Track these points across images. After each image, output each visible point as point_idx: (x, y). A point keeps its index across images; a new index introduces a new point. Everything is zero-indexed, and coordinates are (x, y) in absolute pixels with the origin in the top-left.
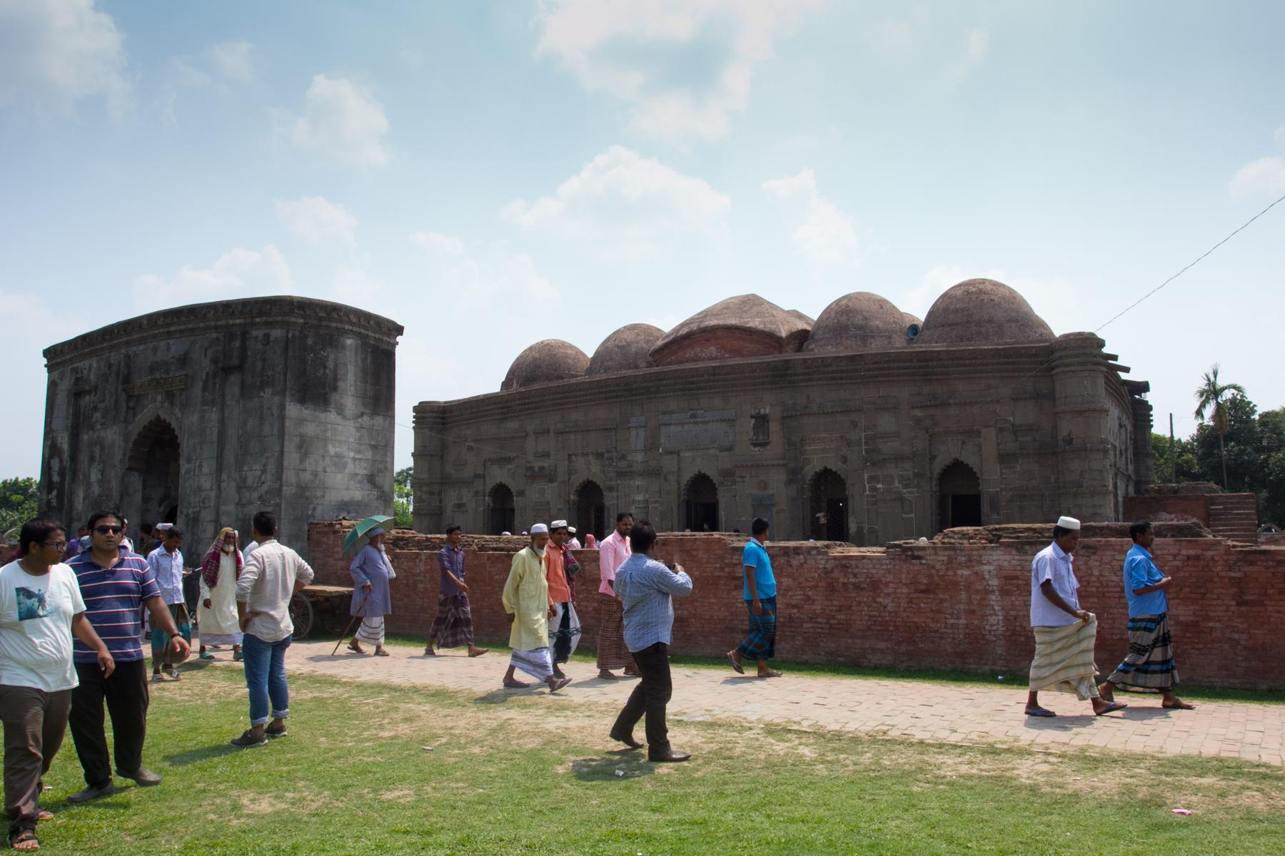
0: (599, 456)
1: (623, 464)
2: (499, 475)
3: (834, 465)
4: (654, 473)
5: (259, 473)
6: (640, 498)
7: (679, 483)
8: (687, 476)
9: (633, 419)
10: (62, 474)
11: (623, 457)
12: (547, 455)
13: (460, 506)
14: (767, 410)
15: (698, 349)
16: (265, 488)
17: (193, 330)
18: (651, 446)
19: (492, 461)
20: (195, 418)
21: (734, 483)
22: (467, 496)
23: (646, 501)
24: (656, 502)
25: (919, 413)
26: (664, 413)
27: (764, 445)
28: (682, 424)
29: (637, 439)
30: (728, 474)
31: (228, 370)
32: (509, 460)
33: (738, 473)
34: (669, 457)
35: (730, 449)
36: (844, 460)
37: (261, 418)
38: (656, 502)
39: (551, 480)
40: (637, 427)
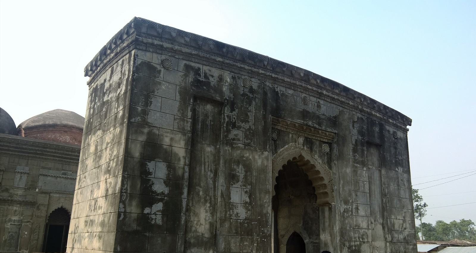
5: (401, 222)
6: (14, 218)
7: (47, 211)
8: (53, 208)
9: (18, 167)
10: (173, 182)
15: (58, 135)
16: (406, 233)
17: (342, 102)
18: (31, 186)
20: (349, 170)
23: (21, 221)
24: (28, 222)
26: (44, 168)
31: (370, 144)
34: (43, 195)
37: (398, 185)
38: (28, 222)
40: (21, 173)
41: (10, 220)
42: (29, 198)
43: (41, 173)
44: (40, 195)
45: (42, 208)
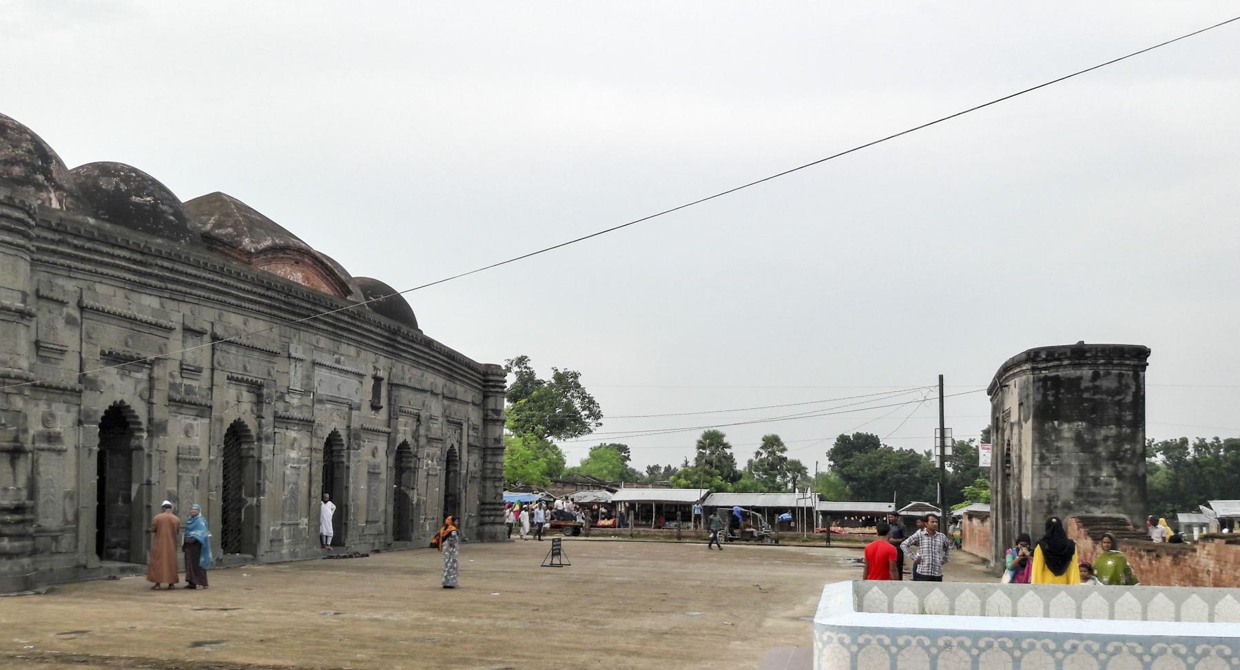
0: (256, 388)
1: (280, 406)
2: (120, 388)
3: (410, 440)
4: (308, 424)
11: (281, 397)
12: (199, 370)
13: (52, 438)
14: (381, 374)
19: (111, 358)
21: (359, 447)
22: (64, 420)
23: (299, 461)
25: (446, 402)
26: (317, 348)
27: (375, 407)
28: (331, 368)
29: (295, 377)
30: (355, 436)
32: (141, 363)
33: (363, 436)
35: (359, 408)
36: (416, 437)
39: (204, 410)
41: (289, 458)
42: (306, 415)
43: (319, 360)
44: (317, 406)
45: (319, 432)
